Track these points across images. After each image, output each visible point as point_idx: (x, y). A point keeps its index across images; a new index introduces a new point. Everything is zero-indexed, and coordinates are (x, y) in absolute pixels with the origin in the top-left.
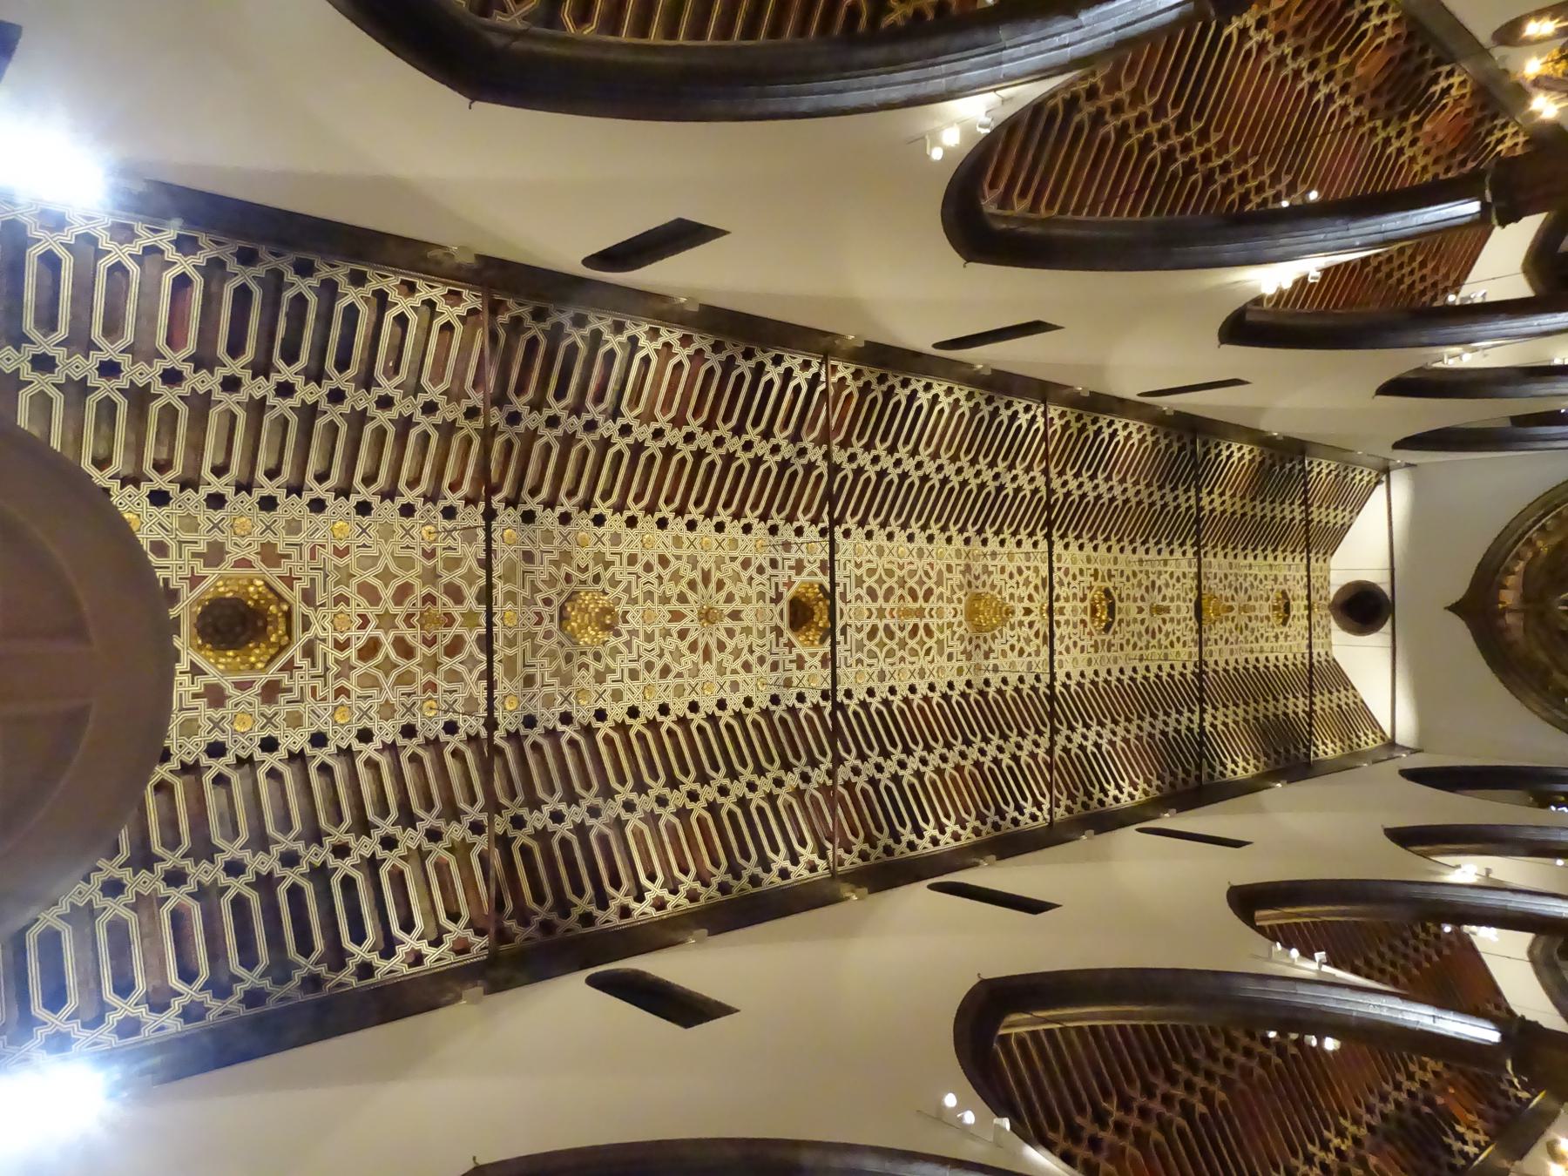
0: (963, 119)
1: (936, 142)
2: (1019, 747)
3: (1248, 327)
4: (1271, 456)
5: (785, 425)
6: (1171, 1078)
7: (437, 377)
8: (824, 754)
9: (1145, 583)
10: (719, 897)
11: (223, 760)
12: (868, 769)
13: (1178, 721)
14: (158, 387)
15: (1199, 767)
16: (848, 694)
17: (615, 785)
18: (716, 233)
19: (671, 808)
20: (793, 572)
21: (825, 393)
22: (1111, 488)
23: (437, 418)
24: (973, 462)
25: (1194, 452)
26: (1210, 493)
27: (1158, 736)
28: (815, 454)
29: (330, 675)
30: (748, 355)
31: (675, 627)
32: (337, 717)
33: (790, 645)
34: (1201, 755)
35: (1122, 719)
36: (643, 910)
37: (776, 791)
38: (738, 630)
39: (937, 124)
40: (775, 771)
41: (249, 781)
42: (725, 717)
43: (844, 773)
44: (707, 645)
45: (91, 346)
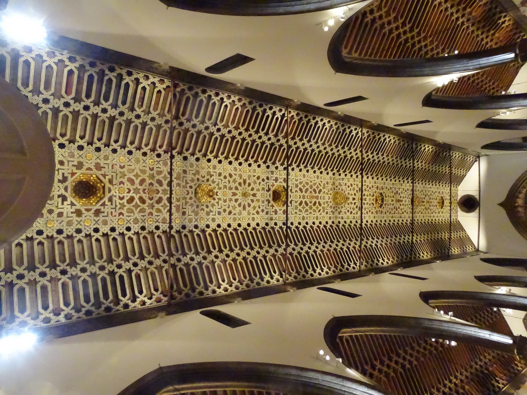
0: (336, 16)
1: (326, 25)
2: (350, 244)
3: (432, 100)
4: (439, 150)
5: (273, 131)
6: (398, 355)
7: (155, 109)
8: (283, 243)
9: (394, 191)
10: (246, 288)
11: (81, 235)
12: (298, 249)
13: (404, 239)
14: (62, 108)
15: (411, 254)
16: (292, 224)
17: (212, 249)
18: (251, 59)
19: (231, 258)
20: (274, 182)
21: (286, 120)
22: (383, 158)
23: (155, 123)
24: (337, 147)
25: (412, 147)
26: (418, 161)
27: (397, 243)
28: (283, 141)
29: (117, 208)
30: (261, 106)
31: (234, 198)
32: (119, 222)
33: (273, 206)
34: (412, 250)
35: (385, 237)
36: (220, 291)
37: (266, 254)
38: (255, 200)
39: (326, 18)
40: (266, 248)
41: (89, 242)
42: (250, 229)
43: (289, 250)
45: (40, 93)
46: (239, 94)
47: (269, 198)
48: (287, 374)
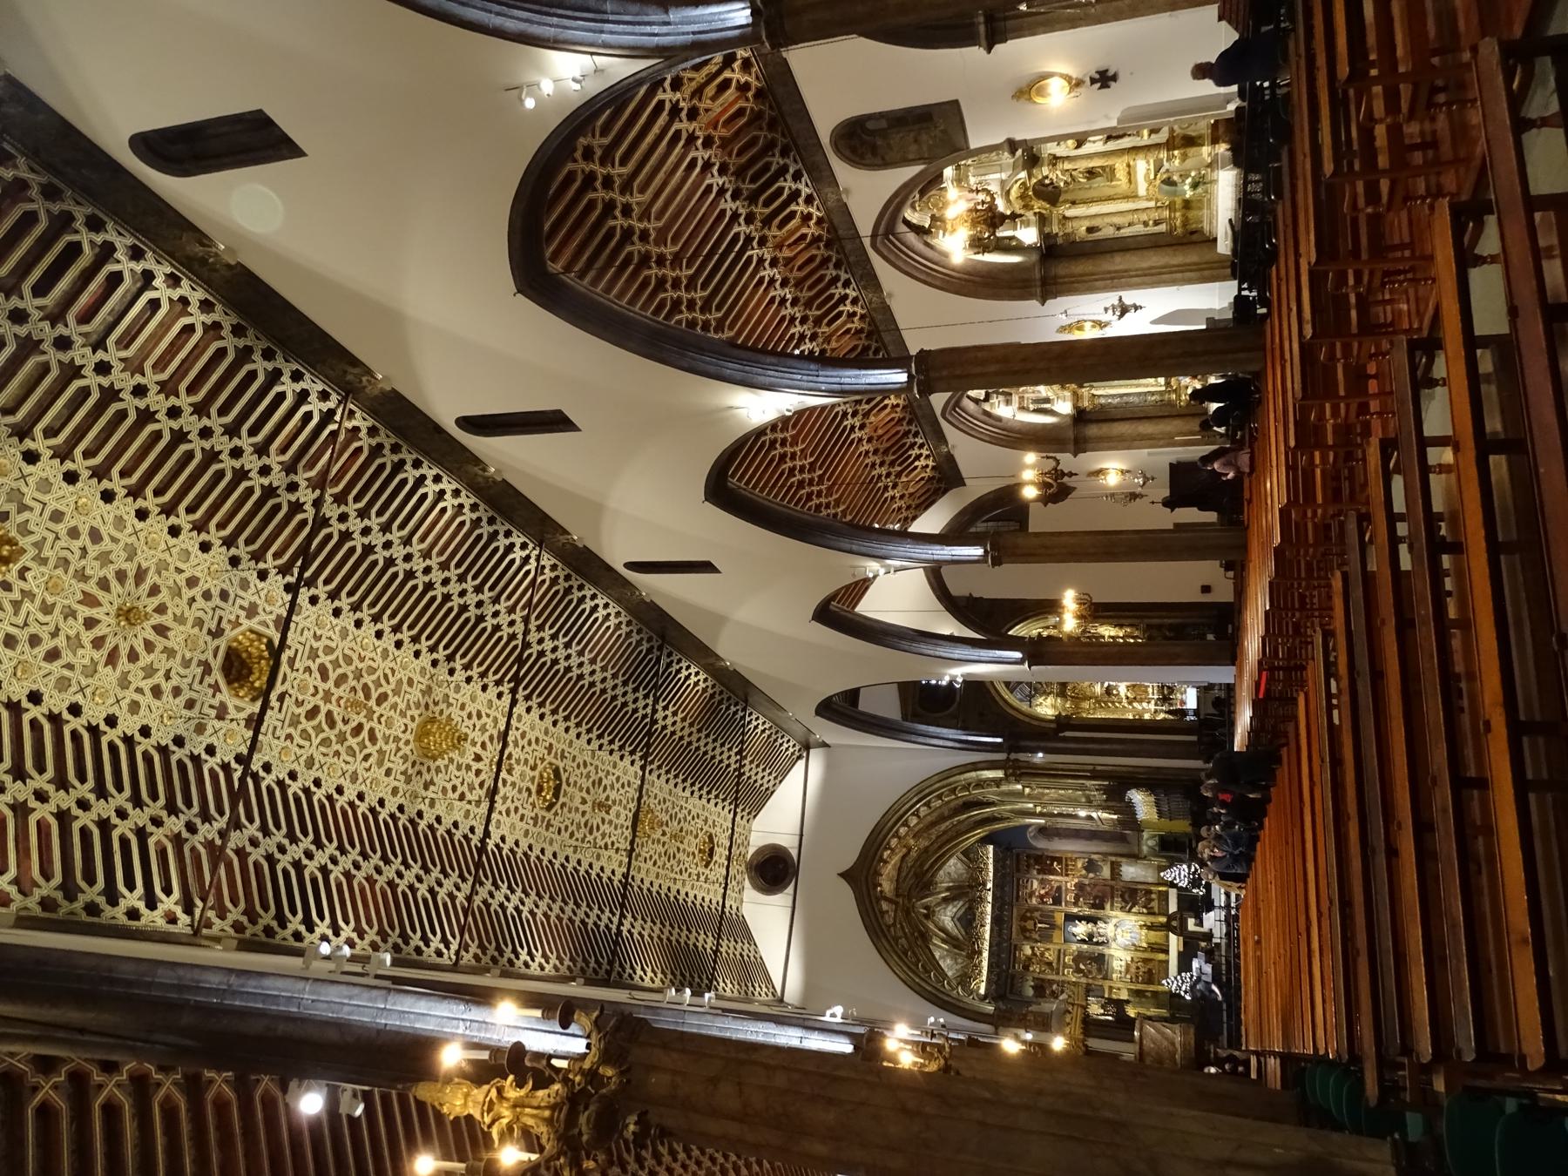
2: (440, 884)
4: (721, 693)
5: (283, 450)
8: (222, 814)
12: (269, 845)
15: (611, 963)
16: (267, 767)
20: (243, 614)
21: (334, 434)
22: (581, 665)
24: (462, 578)
26: (665, 708)
27: (577, 923)
28: (306, 496)
30: (268, 355)
31: (84, 612)
33: (216, 688)
34: (614, 953)
42: (110, 735)
43: (236, 839)
44: (116, 648)
46: (207, 284)
47: (211, 660)
48: (180, 988)
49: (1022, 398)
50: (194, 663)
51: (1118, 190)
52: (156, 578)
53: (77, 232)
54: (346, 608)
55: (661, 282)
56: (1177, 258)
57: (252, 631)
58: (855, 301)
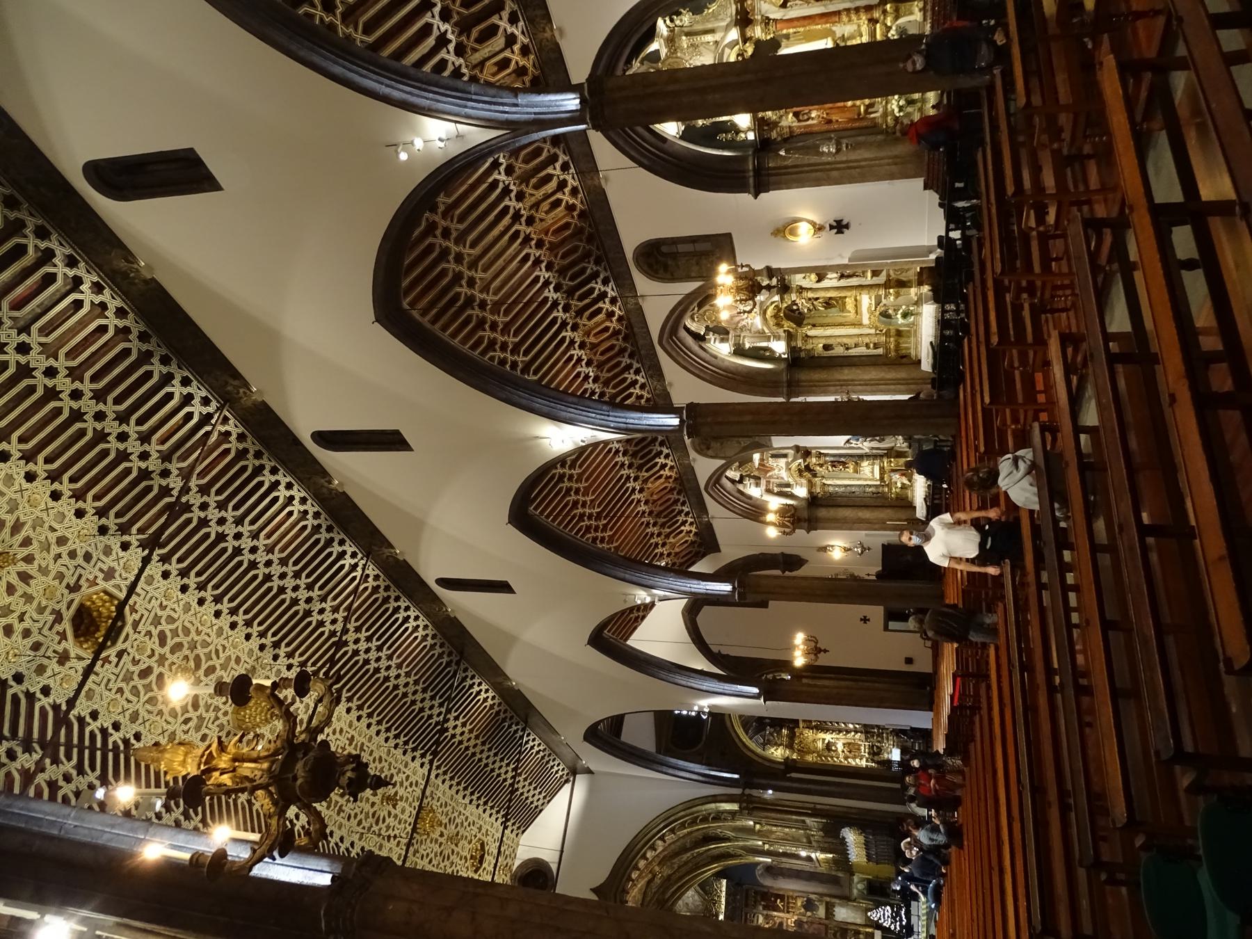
4: (505, 711)
5: (163, 441)
20: (101, 576)
24: (297, 575)
26: (456, 718)
28: (175, 483)
30: (165, 361)
33: (63, 636)
46: (125, 293)
47: (64, 611)
49: (768, 482)
50: (48, 610)
51: (848, 319)
52: (31, 533)
53: (26, 237)
54: (193, 586)
55: (492, 343)
56: (892, 375)
57: (106, 592)
58: (643, 387)
